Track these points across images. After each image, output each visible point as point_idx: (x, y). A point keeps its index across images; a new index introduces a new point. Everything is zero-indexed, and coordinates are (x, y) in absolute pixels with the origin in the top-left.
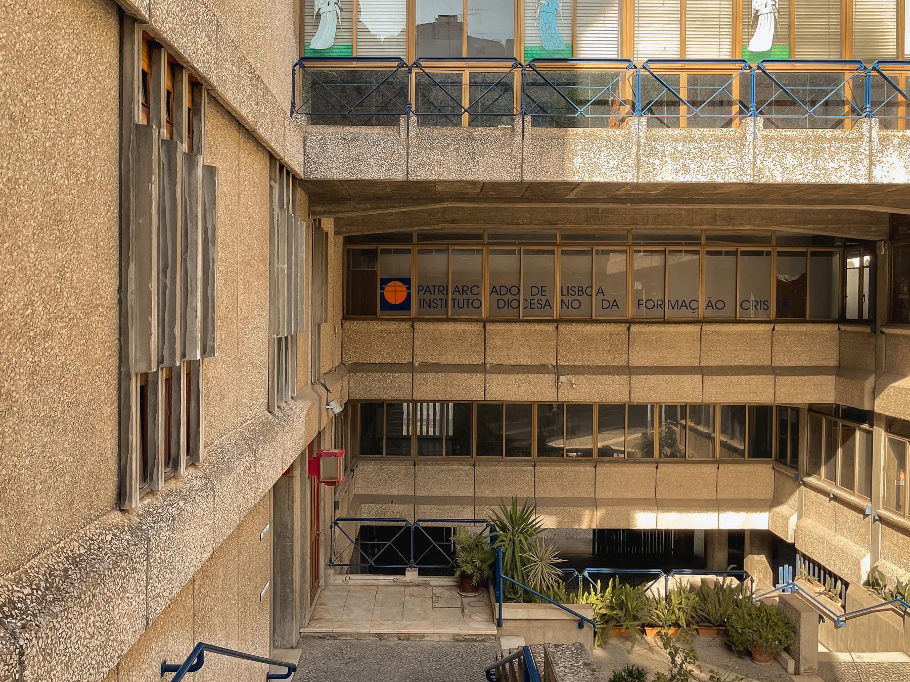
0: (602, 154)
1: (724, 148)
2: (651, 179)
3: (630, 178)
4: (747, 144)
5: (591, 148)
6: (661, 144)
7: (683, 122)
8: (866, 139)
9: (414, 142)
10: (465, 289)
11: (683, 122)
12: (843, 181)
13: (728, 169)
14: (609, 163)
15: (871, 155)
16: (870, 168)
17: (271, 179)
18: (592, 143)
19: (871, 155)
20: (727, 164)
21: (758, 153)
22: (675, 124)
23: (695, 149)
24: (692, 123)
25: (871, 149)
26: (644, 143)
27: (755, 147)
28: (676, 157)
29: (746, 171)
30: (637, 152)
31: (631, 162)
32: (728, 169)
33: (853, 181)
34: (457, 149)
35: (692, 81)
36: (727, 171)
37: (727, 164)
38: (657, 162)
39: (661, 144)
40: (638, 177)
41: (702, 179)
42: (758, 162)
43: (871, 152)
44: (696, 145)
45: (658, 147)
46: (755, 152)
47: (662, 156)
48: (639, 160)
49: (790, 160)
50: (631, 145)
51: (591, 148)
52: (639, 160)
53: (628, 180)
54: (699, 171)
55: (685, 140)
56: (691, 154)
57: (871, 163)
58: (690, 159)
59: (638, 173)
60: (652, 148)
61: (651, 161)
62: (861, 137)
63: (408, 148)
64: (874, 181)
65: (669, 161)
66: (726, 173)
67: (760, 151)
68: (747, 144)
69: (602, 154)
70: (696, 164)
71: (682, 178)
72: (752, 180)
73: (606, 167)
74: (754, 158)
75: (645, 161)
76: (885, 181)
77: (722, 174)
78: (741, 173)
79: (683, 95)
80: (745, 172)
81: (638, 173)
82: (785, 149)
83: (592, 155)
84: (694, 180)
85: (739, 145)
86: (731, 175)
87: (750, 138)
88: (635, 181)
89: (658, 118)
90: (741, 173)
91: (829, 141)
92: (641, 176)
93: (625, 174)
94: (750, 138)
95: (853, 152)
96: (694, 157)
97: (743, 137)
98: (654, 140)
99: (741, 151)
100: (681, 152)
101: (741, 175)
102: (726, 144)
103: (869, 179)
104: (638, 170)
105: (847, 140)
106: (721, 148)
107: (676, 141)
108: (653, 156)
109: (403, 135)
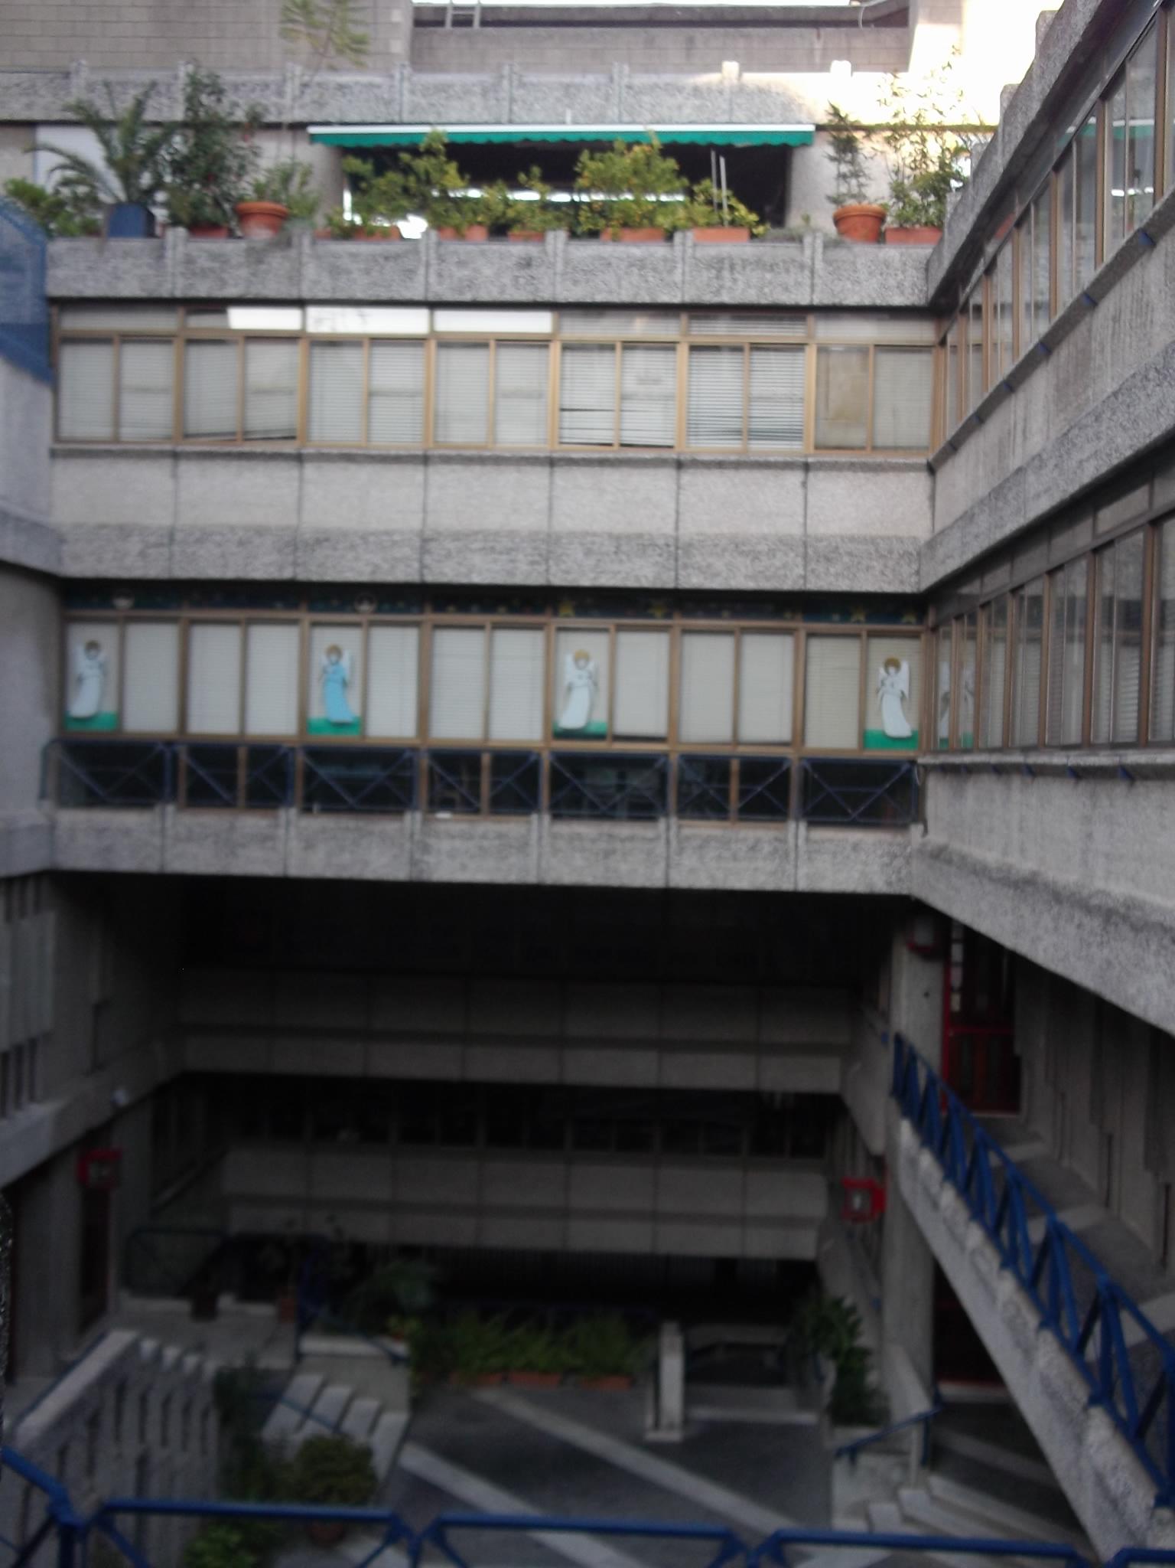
8: (663, 841)
49: (578, 860)
55: (467, 837)
57: (668, 866)
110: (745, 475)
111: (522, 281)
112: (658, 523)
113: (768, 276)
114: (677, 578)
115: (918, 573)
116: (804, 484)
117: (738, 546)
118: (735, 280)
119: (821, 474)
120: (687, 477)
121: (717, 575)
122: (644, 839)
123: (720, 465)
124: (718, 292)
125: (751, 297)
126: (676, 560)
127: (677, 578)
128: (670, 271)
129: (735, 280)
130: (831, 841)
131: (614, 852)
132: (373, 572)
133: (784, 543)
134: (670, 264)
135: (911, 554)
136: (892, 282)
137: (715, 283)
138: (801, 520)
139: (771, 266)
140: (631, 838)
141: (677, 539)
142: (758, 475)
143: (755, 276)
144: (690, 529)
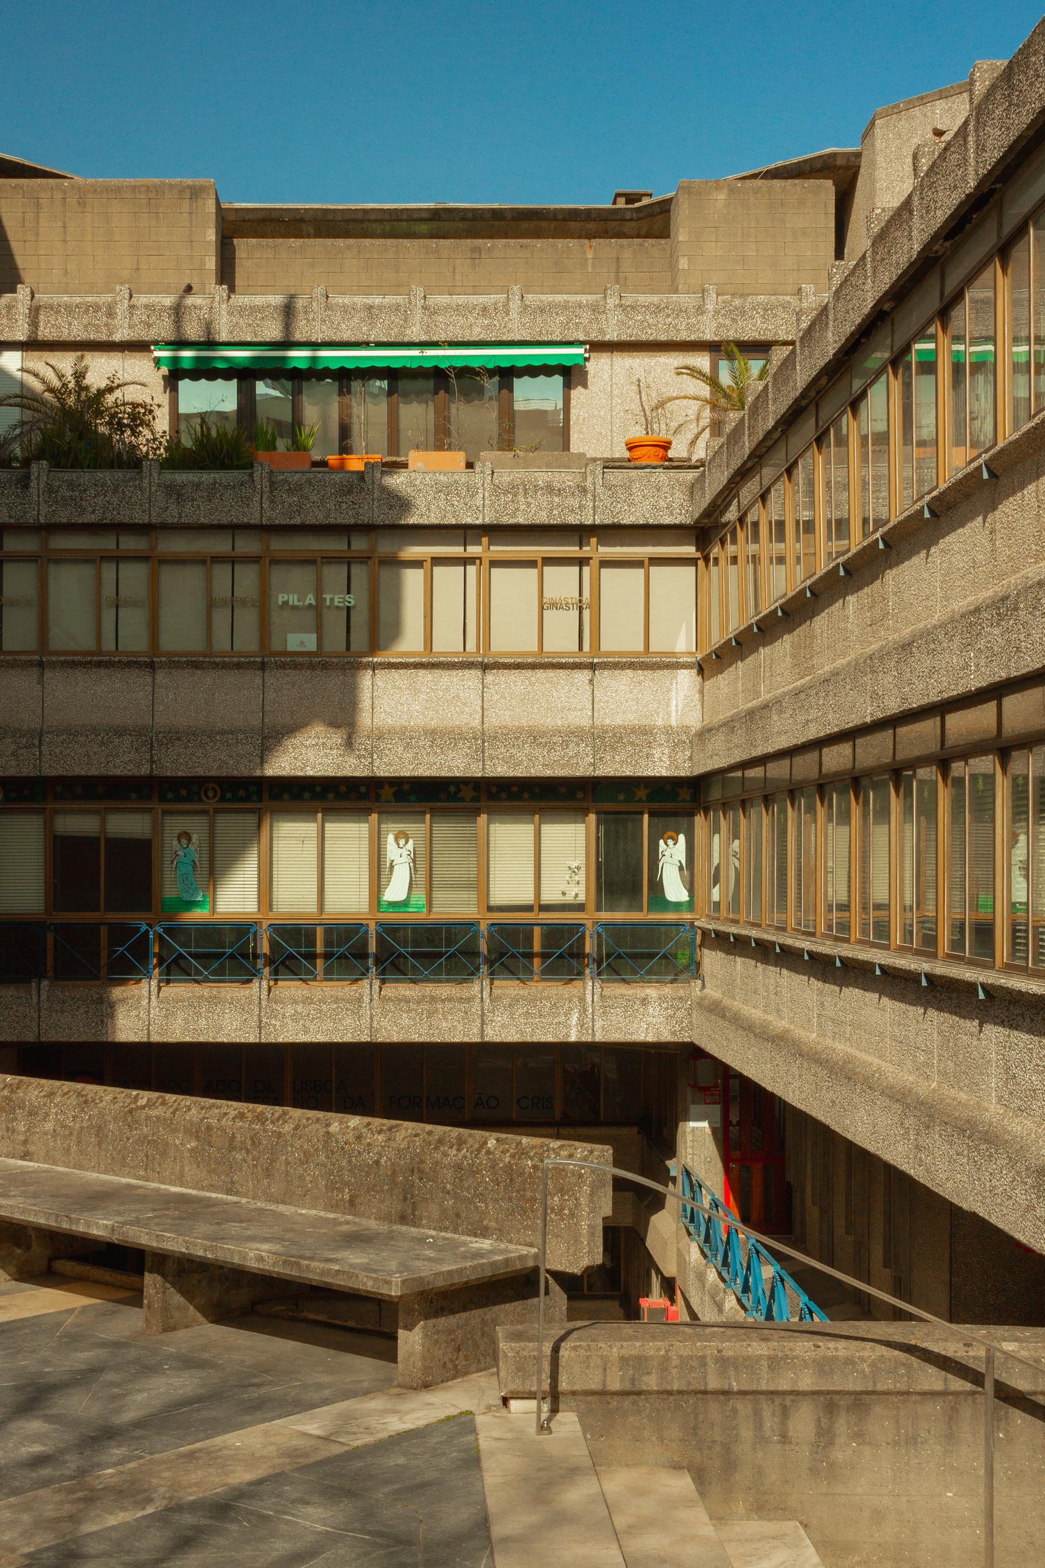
0: (226, 1016)
2: (272, 1039)
3: (252, 1039)
8: (478, 1000)
9: (45, 1005)
12: (456, 1040)
15: (483, 1015)
16: (482, 1027)
19: (483, 1015)
25: (482, 1010)
27: (371, 1008)
30: (259, 1015)
33: (466, 1040)
41: (321, 1038)
42: (375, 1023)
43: (483, 1012)
46: (371, 1014)
48: (260, 1022)
49: (405, 1020)
52: (260, 1022)
55: (307, 1001)
57: (483, 1023)
61: (273, 1022)
62: (473, 998)
63: (39, 1011)
64: (487, 1039)
69: (226, 1016)
74: (371, 1018)
76: (498, 1039)
80: (362, 1032)
82: (401, 1010)
83: (216, 1017)
84: (314, 1040)
87: (366, 999)
88: (257, 1040)
91: (443, 1001)
94: (366, 999)
95: (466, 1013)
97: (360, 1000)
103: (482, 1037)
105: (461, 1000)
107: (296, 1002)
109: (35, 999)
110: (540, 673)
111: (344, 506)
112: (467, 717)
113: (556, 499)
114: (484, 769)
115: (691, 758)
116: (591, 681)
117: (536, 736)
118: (529, 504)
119: (606, 673)
120: (490, 677)
121: (520, 763)
122: (461, 1000)
123: (518, 666)
124: (513, 515)
125: (543, 518)
126: (483, 752)
127: (484, 769)
128: (472, 496)
129: (529, 504)
130: (623, 996)
131: (436, 1011)
132: (220, 768)
133: (577, 734)
134: (472, 490)
135: (684, 742)
136: (662, 504)
137: (511, 507)
138: (590, 713)
139: (559, 490)
140: (449, 999)
141: (483, 734)
142: (551, 673)
143: (543, 499)
144: (493, 721)
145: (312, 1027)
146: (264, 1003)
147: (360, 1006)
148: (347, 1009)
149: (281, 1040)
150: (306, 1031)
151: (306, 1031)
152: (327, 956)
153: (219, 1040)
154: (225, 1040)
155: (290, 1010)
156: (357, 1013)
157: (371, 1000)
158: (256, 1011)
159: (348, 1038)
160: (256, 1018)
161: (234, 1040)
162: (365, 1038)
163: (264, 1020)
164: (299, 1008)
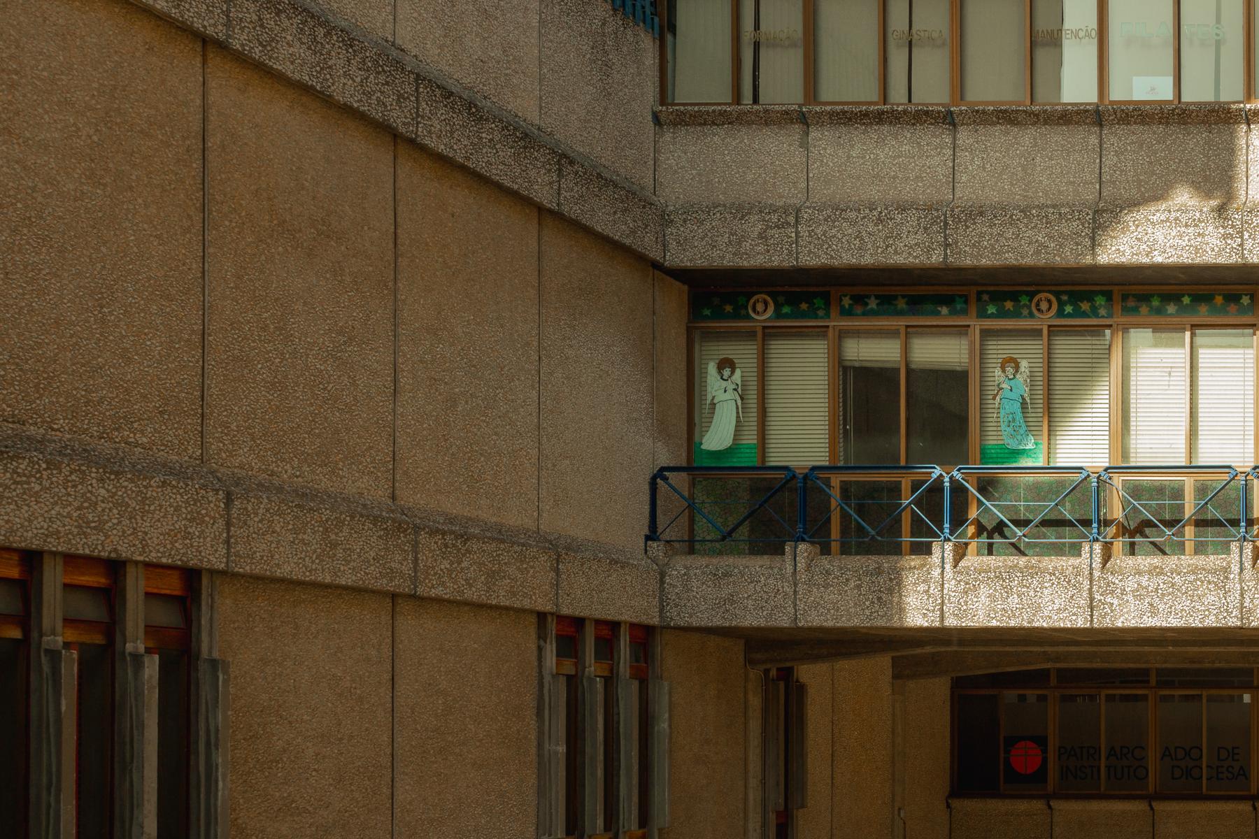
0: (1046, 592)
1: (1202, 582)
2: (1107, 623)
3: (1081, 623)
4: (1232, 576)
5: (1030, 584)
6: (1120, 577)
7: (1189, 546)
10: (1125, 751)
11: (1189, 546)
13: (1208, 610)
14: (1054, 603)
17: (539, 638)
18: (1032, 577)
20: (1206, 603)
21: (1246, 588)
22: (1180, 548)
23: (1164, 583)
24: (1200, 549)
26: (1099, 577)
27: (1241, 581)
28: (1140, 595)
29: (1232, 612)
30: (1090, 590)
31: (1082, 602)
32: (1208, 610)
34: (859, 587)
35: (1201, 490)
36: (1207, 613)
37: (1206, 603)
38: (1116, 602)
39: (1120, 577)
40: (1092, 621)
41: (1174, 622)
44: (1166, 578)
45: (1117, 582)
46: (1242, 589)
47: (1122, 594)
48: (1092, 599)
50: (1081, 579)
51: (1030, 584)
53: (1079, 625)
54: (1171, 613)
55: (1156, 571)
56: (1160, 591)
58: (1158, 597)
59: (1092, 616)
60: (1108, 583)
61: (1109, 600)
65: (1130, 598)
66: (1206, 616)
67: (1248, 586)
68: (1232, 576)
69: (1046, 592)
70: (1166, 604)
71: (1149, 622)
72: (1239, 623)
73: (1050, 608)
74: (1242, 595)
75: (1100, 601)
77: (1200, 617)
78: (1225, 614)
79: (1189, 511)
81: (1092, 616)
83: (1032, 593)
84: (1164, 624)
85: (1222, 578)
86: (1213, 618)
88: (1088, 625)
89: (1152, 543)
90: (1225, 614)
92: (1096, 620)
93: (1074, 618)
94: (1235, 568)
96: (1163, 595)
97: (1226, 570)
98: (1112, 573)
99: (1224, 587)
100: (1146, 588)
101: (1225, 618)
102: (1205, 577)
104: (1092, 612)
106: (1199, 583)
107: (1139, 573)
108: (1110, 593)
145: (1161, 607)
146: (1096, 574)
147: (1227, 578)
148: (1209, 582)
149: (1120, 625)
150: (1154, 611)
151: (1154, 611)
152: (1201, 523)
153: (1036, 624)
154: (1045, 625)
155: (1131, 584)
156: (1222, 587)
157: (1242, 570)
158: (1086, 583)
159: (1211, 622)
160: (1085, 594)
161: (1057, 625)
162: (1234, 622)
163: (1097, 597)
164: (1144, 580)
